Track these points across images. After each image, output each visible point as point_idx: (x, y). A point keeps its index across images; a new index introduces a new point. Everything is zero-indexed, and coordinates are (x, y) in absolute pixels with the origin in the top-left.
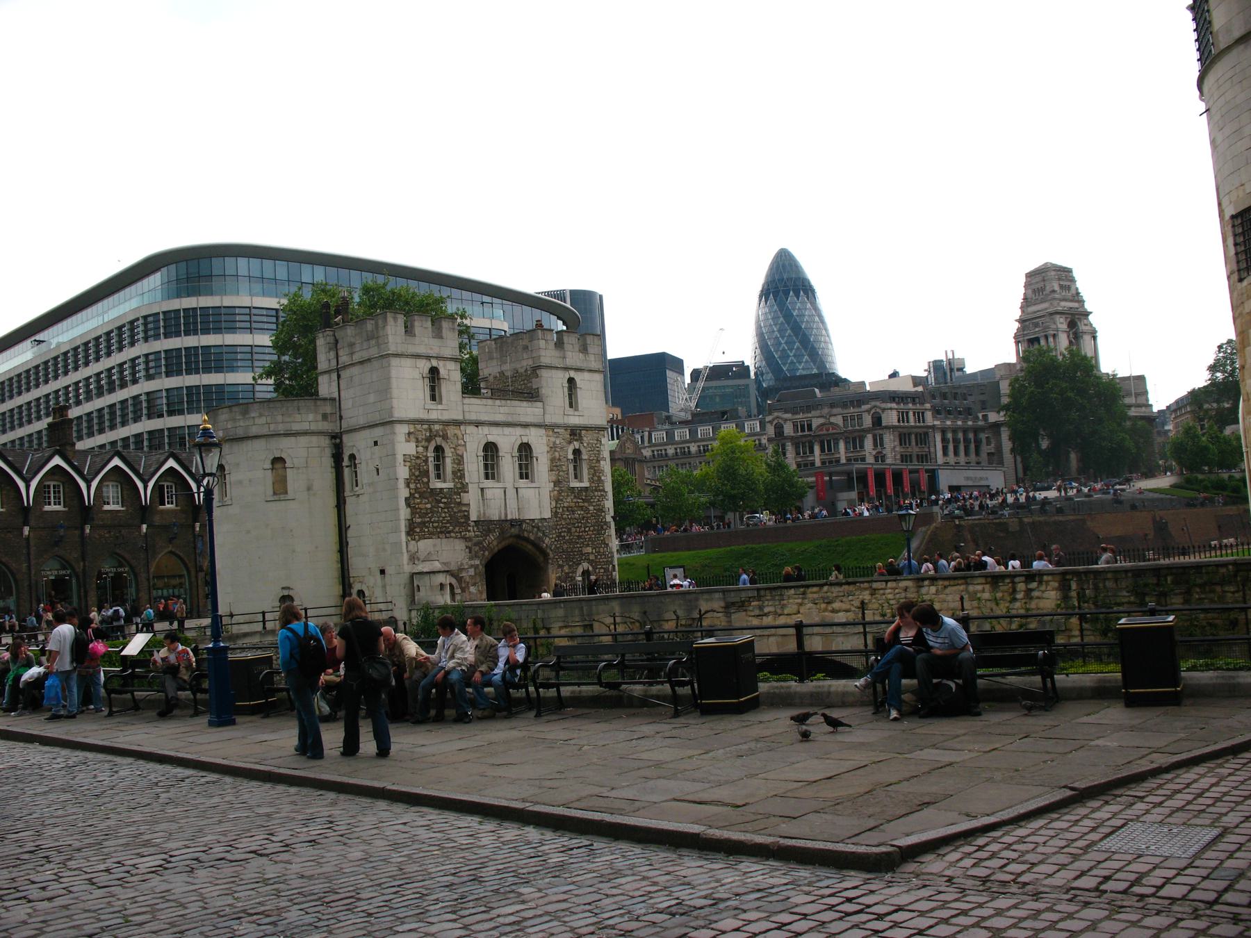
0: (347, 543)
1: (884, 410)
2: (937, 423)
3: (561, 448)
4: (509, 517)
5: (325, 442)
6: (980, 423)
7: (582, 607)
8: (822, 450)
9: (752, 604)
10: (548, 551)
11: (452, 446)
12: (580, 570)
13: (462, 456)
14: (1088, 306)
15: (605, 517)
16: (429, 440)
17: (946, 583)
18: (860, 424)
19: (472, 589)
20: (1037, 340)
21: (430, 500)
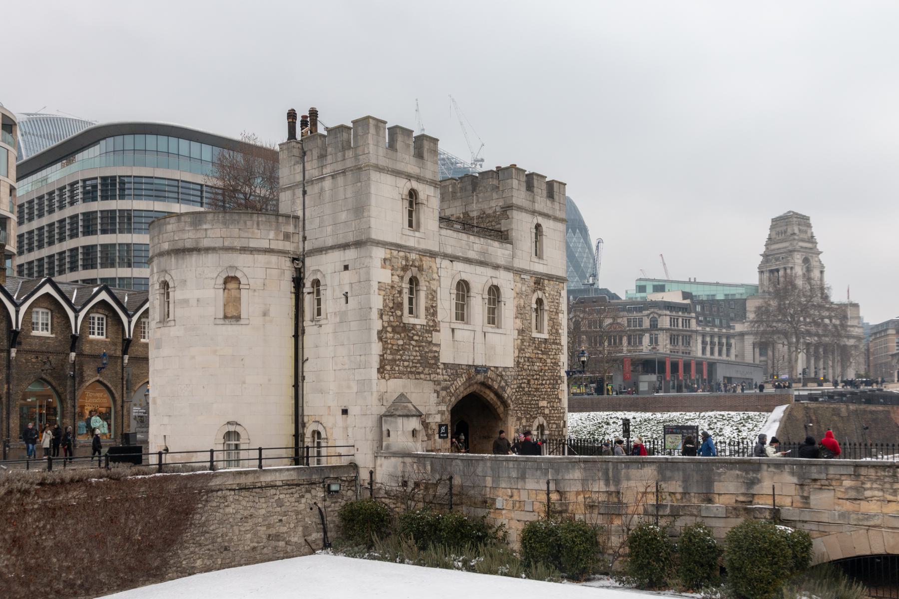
0: (303, 378)
1: (660, 315)
2: (699, 328)
5: (286, 263)
10: (509, 401)
11: (426, 279)
12: (536, 424)
13: (435, 292)
14: (820, 247)
15: (559, 371)
16: (405, 269)
18: (640, 325)
20: (778, 271)
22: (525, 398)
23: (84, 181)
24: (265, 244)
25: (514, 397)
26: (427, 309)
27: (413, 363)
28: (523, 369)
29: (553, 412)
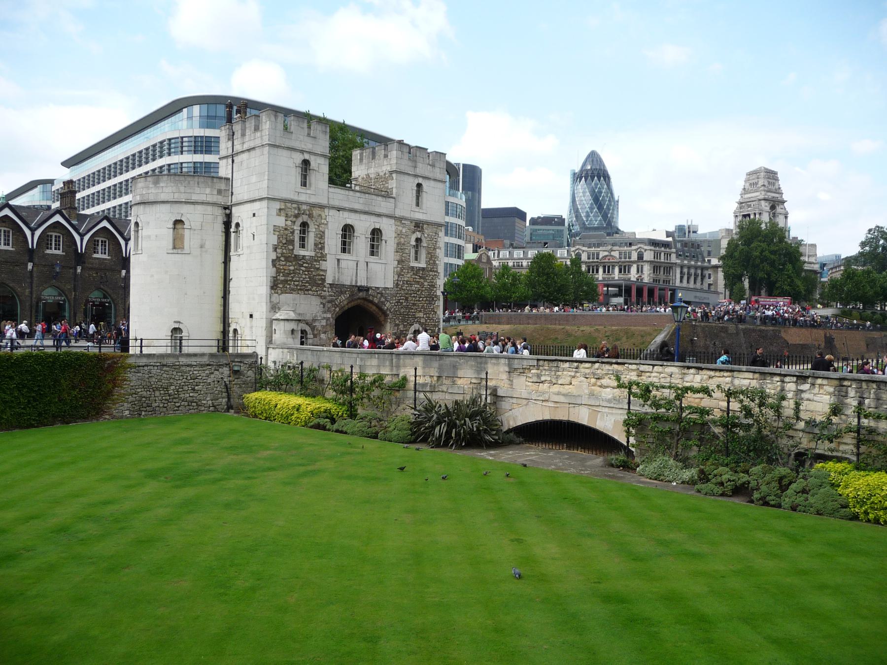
0: (229, 291)
1: (646, 250)
2: (678, 261)
3: (406, 236)
4: (359, 284)
5: (219, 213)
6: (706, 264)
7: (392, 360)
8: (604, 272)
9: (532, 371)
11: (316, 223)
12: (412, 329)
13: (324, 233)
14: (785, 197)
15: (436, 291)
16: (297, 216)
17: (712, 373)
18: (630, 258)
19: (323, 336)
20: (749, 215)
21: (294, 263)
22: (402, 310)
23: (170, 140)
24: (203, 198)
25: (393, 309)
26: (316, 245)
27: (302, 283)
28: (401, 289)
29: (428, 321)
